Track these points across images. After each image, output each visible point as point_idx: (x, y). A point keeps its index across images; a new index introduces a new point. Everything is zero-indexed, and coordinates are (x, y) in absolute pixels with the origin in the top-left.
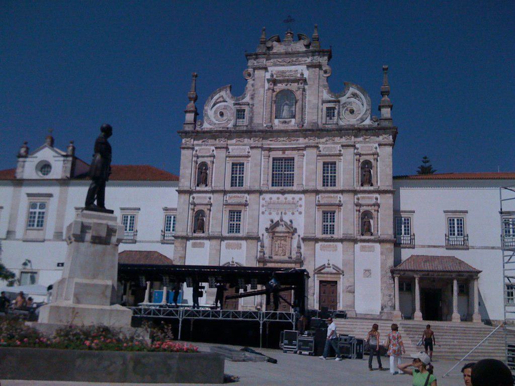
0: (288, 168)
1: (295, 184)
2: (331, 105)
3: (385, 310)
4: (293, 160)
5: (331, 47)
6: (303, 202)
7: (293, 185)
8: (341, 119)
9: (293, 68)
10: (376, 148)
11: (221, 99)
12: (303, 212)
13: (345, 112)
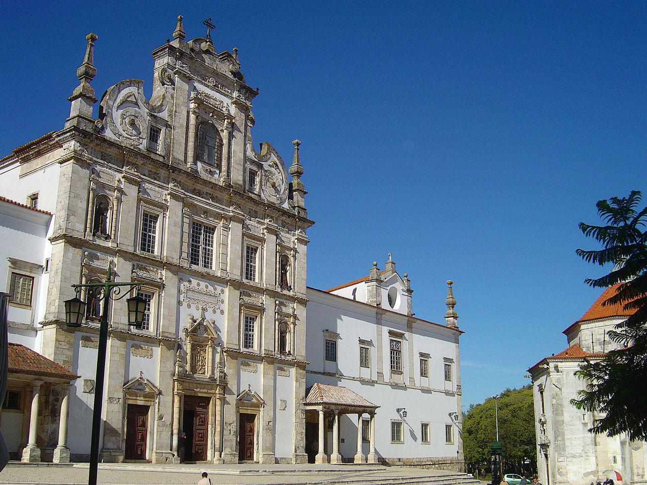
2: (255, 168)
3: (298, 453)
5: (258, 89)
11: (132, 99)
12: (226, 312)
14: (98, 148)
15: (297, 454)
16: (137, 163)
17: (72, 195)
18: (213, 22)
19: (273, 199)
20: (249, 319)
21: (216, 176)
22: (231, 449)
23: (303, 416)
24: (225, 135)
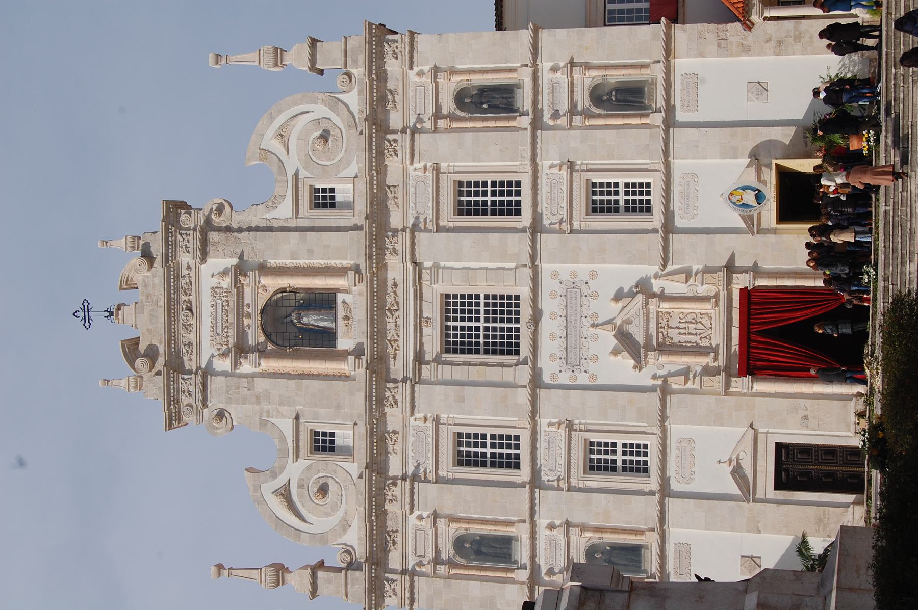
0: (470, 312)
1: (513, 292)
4: (447, 296)
6: (565, 269)
7: (517, 297)
10: (420, 74)
18: (78, 306)
21: (348, 298)
24: (273, 283)
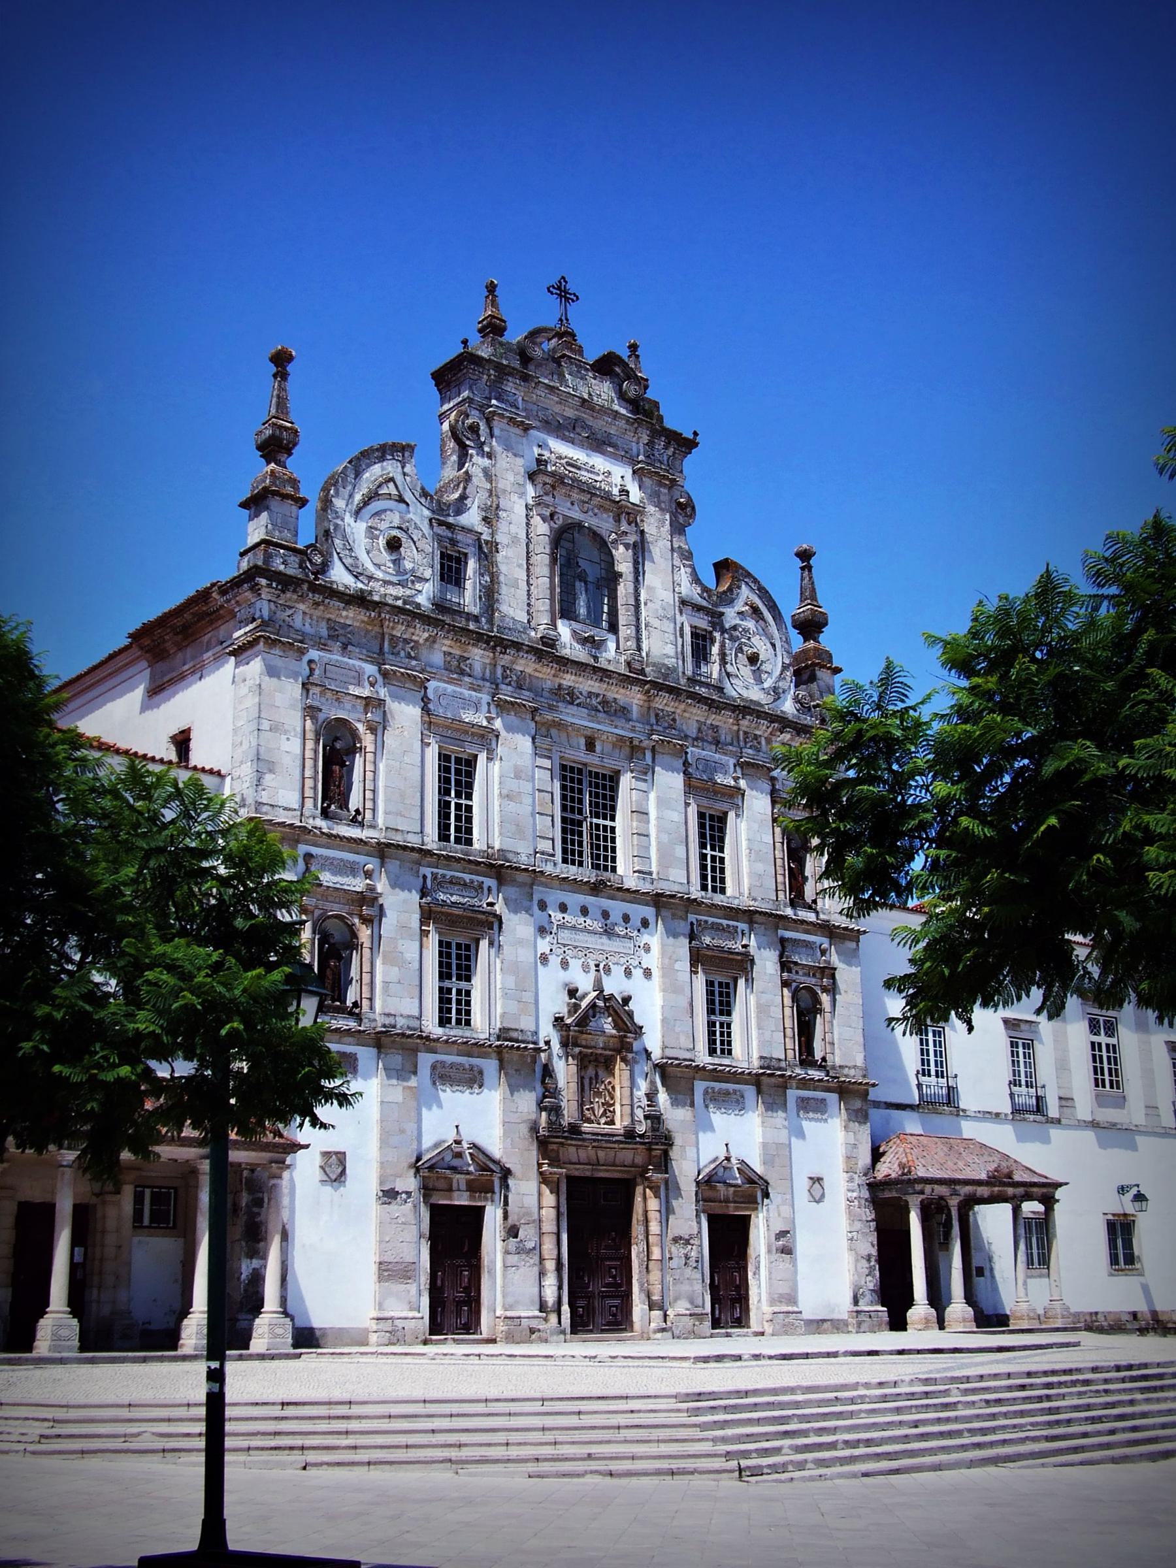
5: (696, 434)
8: (729, 675)
9: (599, 462)
11: (391, 489)
12: (656, 973)
13: (736, 656)
14: (317, 613)
15: (859, 1308)
16: (414, 638)
17: (265, 725)
18: (571, 287)
19: (755, 694)
20: (716, 985)
22: (692, 1302)
23: (868, 1213)
